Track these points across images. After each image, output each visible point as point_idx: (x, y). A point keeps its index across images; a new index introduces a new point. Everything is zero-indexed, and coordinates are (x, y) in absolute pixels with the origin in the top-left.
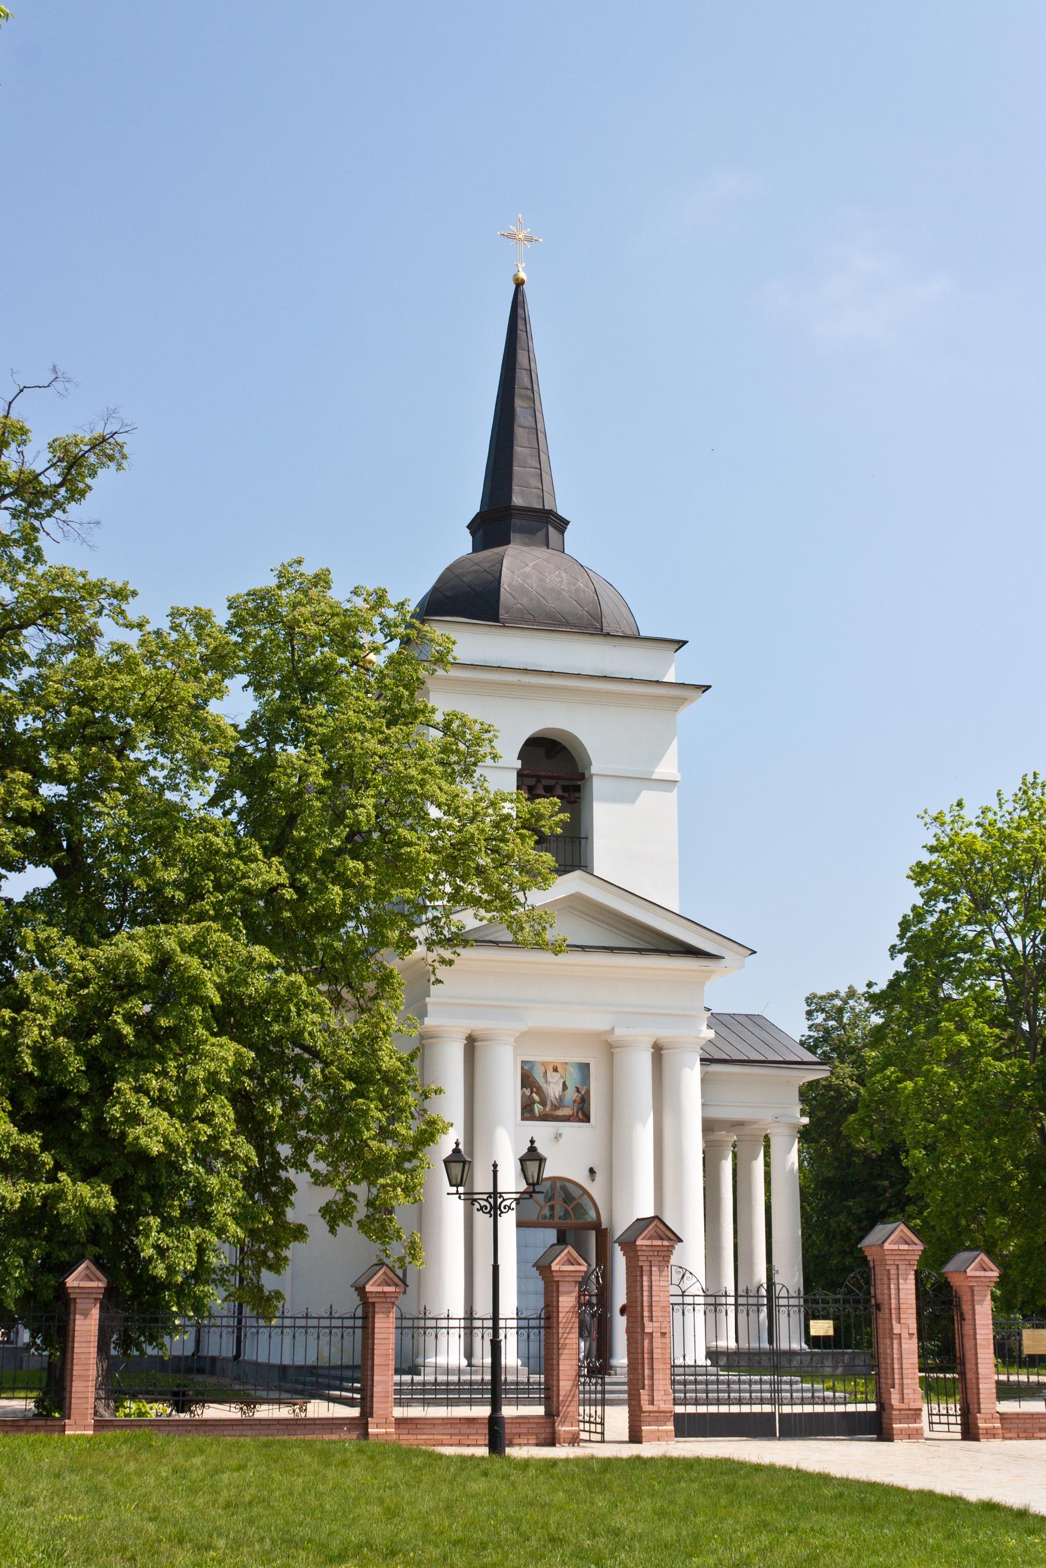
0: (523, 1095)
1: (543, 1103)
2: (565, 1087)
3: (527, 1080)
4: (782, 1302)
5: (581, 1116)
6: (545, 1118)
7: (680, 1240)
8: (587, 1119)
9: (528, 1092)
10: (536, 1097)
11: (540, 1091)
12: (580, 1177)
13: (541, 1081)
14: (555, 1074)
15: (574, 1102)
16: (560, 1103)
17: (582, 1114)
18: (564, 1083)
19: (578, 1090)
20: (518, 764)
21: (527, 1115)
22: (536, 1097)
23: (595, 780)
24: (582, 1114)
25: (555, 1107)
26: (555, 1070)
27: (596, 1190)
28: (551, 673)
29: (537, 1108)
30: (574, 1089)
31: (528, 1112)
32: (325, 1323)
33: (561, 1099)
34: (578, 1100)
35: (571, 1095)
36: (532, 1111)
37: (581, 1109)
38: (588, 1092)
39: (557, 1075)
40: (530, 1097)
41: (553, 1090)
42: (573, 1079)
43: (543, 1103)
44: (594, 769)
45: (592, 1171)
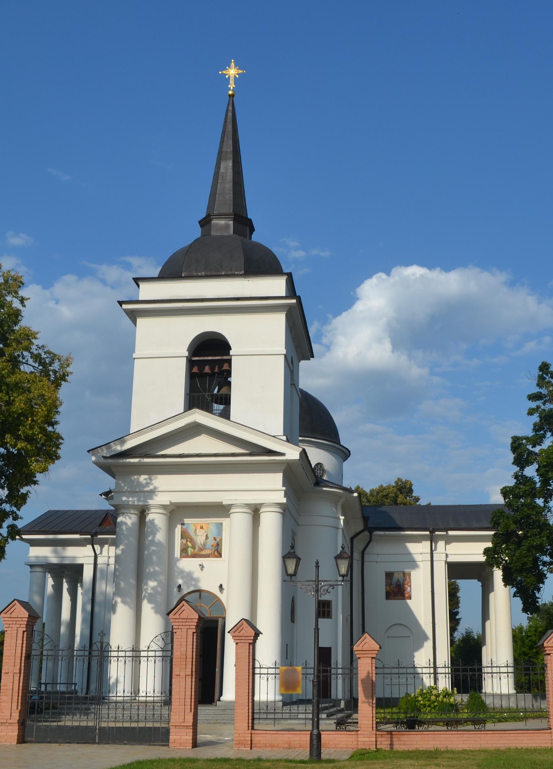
0: (182, 543)
1: (194, 547)
2: (207, 537)
3: (184, 535)
4: (113, 654)
5: (216, 554)
6: (194, 556)
8: (220, 555)
9: (184, 541)
10: (189, 544)
11: (192, 541)
12: (215, 591)
14: (201, 530)
15: (213, 546)
17: (217, 552)
18: (207, 535)
19: (215, 539)
20: (186, 354)
21: (183, 555)
24: (217, 552)
25: (201, 550)
26: (202, 528)
27: (223, 597)
29: (190, 551)
30: (213, 539)
33: (204, 544)
34: (215, 544)
35: (211, 542)
36: (187, 552)
38: (221, 540)
39: (203, 531)
40: (186, 544)
41: (200, 539)
43: (194, 547)
44: (231, 353)
45: (221, 586)
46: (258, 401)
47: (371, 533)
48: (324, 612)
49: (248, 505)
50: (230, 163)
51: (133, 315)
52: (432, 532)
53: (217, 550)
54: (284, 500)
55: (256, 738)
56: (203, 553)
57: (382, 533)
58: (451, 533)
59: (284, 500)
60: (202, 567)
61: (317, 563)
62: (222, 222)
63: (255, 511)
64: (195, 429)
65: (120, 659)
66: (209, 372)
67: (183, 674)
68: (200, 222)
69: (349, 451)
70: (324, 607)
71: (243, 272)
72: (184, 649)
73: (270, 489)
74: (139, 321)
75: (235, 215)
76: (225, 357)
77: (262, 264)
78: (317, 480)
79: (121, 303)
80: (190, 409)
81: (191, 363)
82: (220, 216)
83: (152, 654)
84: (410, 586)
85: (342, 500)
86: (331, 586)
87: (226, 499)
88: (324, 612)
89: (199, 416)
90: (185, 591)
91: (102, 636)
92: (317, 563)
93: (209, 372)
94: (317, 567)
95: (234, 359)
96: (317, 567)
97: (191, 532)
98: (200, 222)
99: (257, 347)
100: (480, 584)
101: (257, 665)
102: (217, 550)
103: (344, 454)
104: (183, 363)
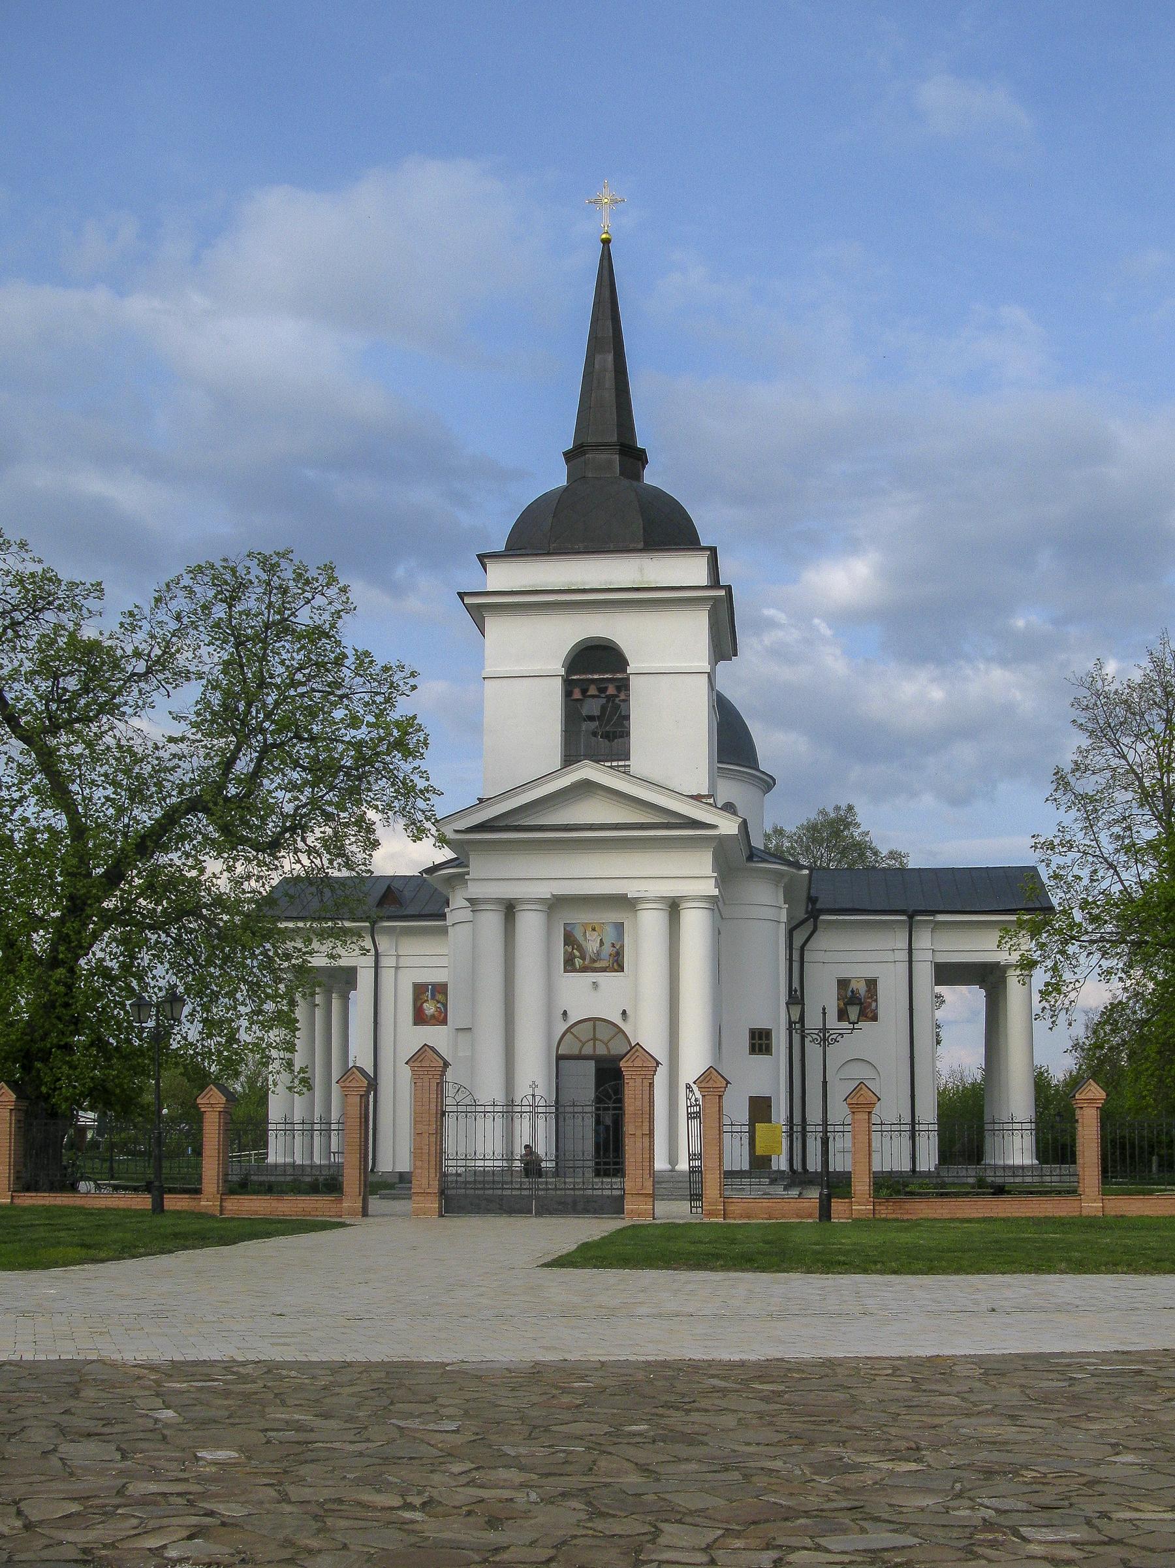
1: (583, 958)
3: (569, 939)
6: (584, 969)
9: (570, 949)
11: (580, 948)
16: (597, 958)
17: (617, 964)
19: (613, 946)
20: (562, 672)
24: (617, 964)
25: (594, 961)
26: (594, 930)
28: (584, 591)
31: (569, 965)
32: (282, 1127)
33: (598, 953)
35: (607, 950)
36: (573, 964)
38: (622, 946)
40: (572, 953)
41: (592, 946)
42: (610, 936)
43: (583, 958)
46: (669, 742)
47: (816, 919)
48: (760, 1045)
49: (663, 899)
50: (610, 358)
51: (478, 614)
52: (911, 917)
53: (617, 961)
54: (716, 892)
55: (731, 1208)
56: (597, 965)
57: (834, 917)
58: (941, 918)
59: (716, 892)
60: (595, 985)
61: (824, 1009)
62: (603, 457)
63: (674, 907)
64: (586, 787)
66: (596, 699)
67: (639, 1133)
68: (565, 454)
69: (774, 780)
70: (760, 1039)
71: (641, 546)
72: (639, 1103)
73: (692, 875)
74: (491, 623)
75: (622, 445)
76: (619, 676)
77: (668, 529)
78: (751, 851)
79: (461, 595)
81: (569, 685)
82: (599, 447)
84: (876, 1001)
85: (786, 880)
87: (632, 889)
88: (760, 1045)
89: (588, 771)
90: (573, 1018)
92: (824, 1009)
93: (596, 699)
94: (824, 1014)
95: (634, 682)
96: (824, 1014)
97: (579, 935)
98: (565, 454)
99: (667, 659)
100: (983, 992)
101: (726, 1121)
102: (617, 961)
103: (767, 783)
104: (558, 684)
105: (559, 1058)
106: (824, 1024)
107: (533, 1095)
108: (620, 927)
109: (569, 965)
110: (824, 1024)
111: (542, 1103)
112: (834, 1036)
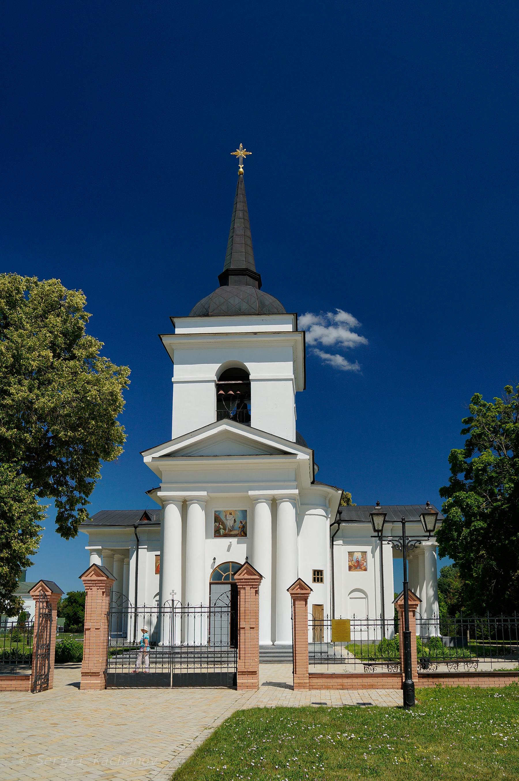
0: (215, 526)
1: (225, 529)
3: (217, 519)
5: (242, 534)
6: (225, 536)
7: (312, 590)
8: (245, 535)
9: (217, 524)
10: (221, 527)
11: (223, 524)
13: (223, 519)
16: (233, 529)
19: (241, 522)
22: (221, 527)
23: (252, 383)
25: (231, 531)
26: (231, 514)
29: (222, 531)
34: (241, 526)
35: (238, 525)
36: (219, 533)
37: (243, 531)
38: (246, 523)
39: (232, 516)
41: (229, 523)
42: (239, 517)
43: (225, 529)
53: (243, 531)
56: (232, 533)
65: (190, 614)
66: (234, 394)
80: (221, 419)
83: (219, 610)
86: (418, 541)
91: (173, 595)
93: (234, 394)
105: (211, 584)
106: (404, 532)
107: (173, 600)
108: (245, 512)
109: (217, 534)
110: (404, 532)
111: (179, 605)
112: (413, 543)
